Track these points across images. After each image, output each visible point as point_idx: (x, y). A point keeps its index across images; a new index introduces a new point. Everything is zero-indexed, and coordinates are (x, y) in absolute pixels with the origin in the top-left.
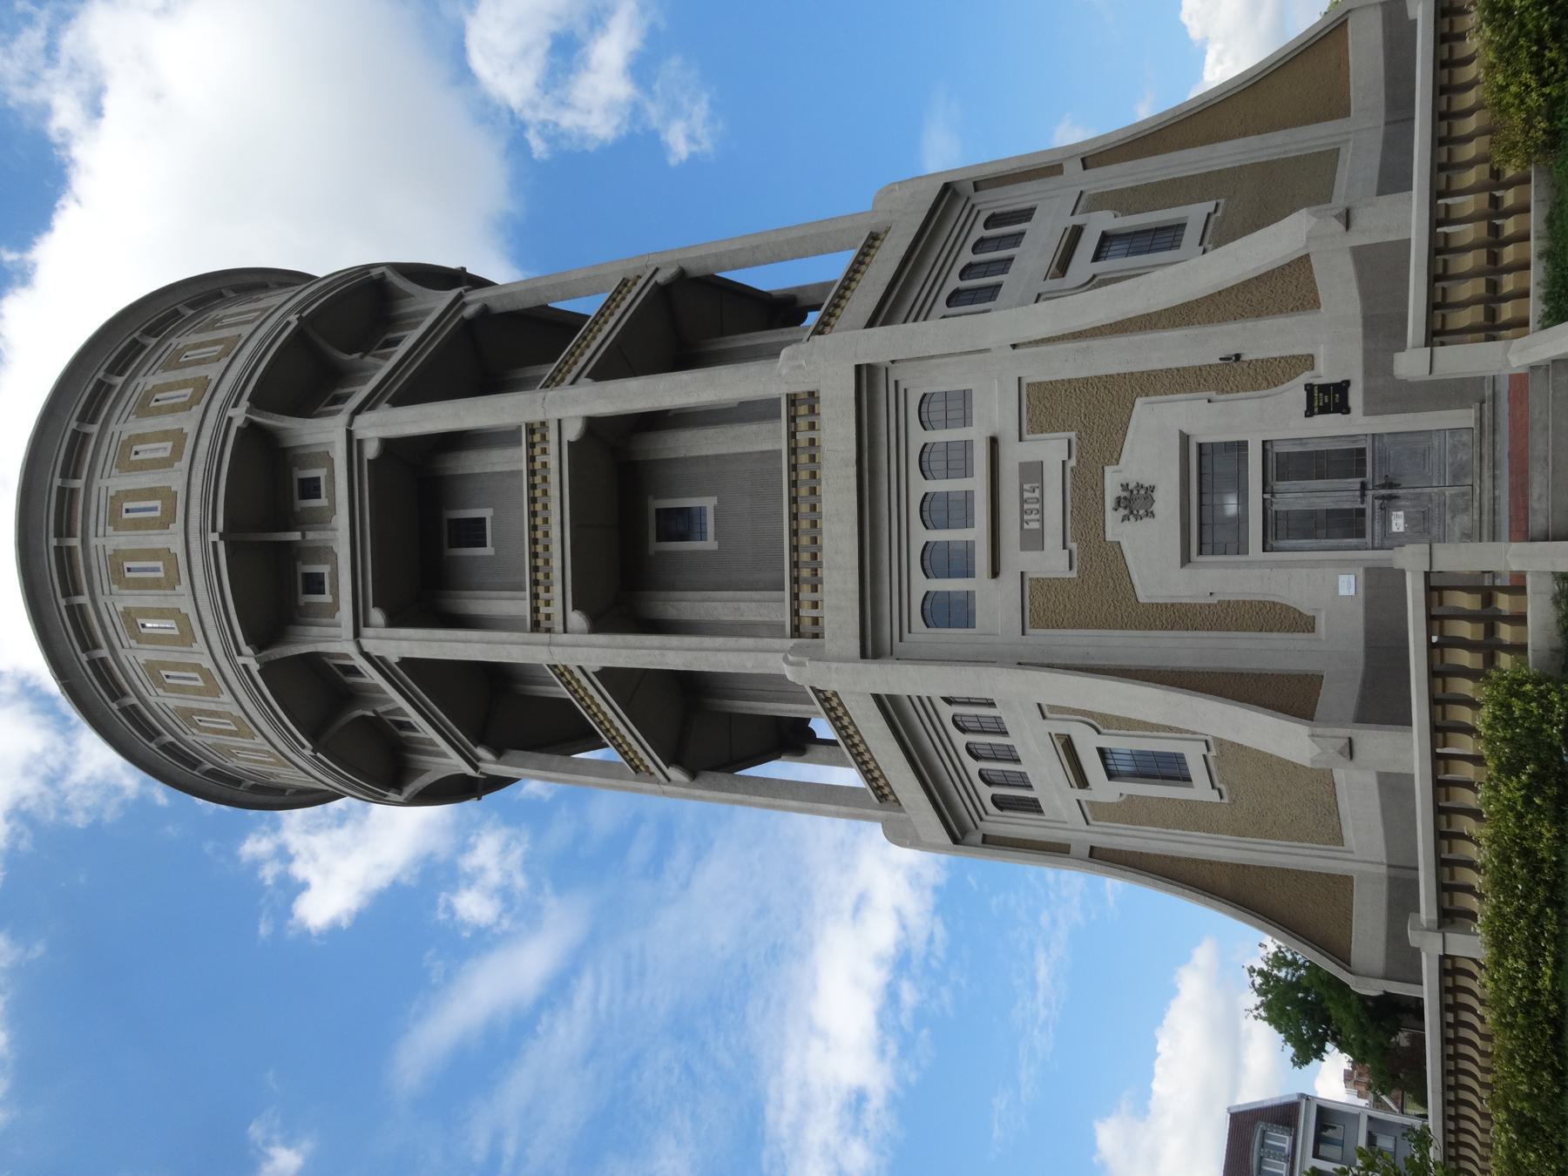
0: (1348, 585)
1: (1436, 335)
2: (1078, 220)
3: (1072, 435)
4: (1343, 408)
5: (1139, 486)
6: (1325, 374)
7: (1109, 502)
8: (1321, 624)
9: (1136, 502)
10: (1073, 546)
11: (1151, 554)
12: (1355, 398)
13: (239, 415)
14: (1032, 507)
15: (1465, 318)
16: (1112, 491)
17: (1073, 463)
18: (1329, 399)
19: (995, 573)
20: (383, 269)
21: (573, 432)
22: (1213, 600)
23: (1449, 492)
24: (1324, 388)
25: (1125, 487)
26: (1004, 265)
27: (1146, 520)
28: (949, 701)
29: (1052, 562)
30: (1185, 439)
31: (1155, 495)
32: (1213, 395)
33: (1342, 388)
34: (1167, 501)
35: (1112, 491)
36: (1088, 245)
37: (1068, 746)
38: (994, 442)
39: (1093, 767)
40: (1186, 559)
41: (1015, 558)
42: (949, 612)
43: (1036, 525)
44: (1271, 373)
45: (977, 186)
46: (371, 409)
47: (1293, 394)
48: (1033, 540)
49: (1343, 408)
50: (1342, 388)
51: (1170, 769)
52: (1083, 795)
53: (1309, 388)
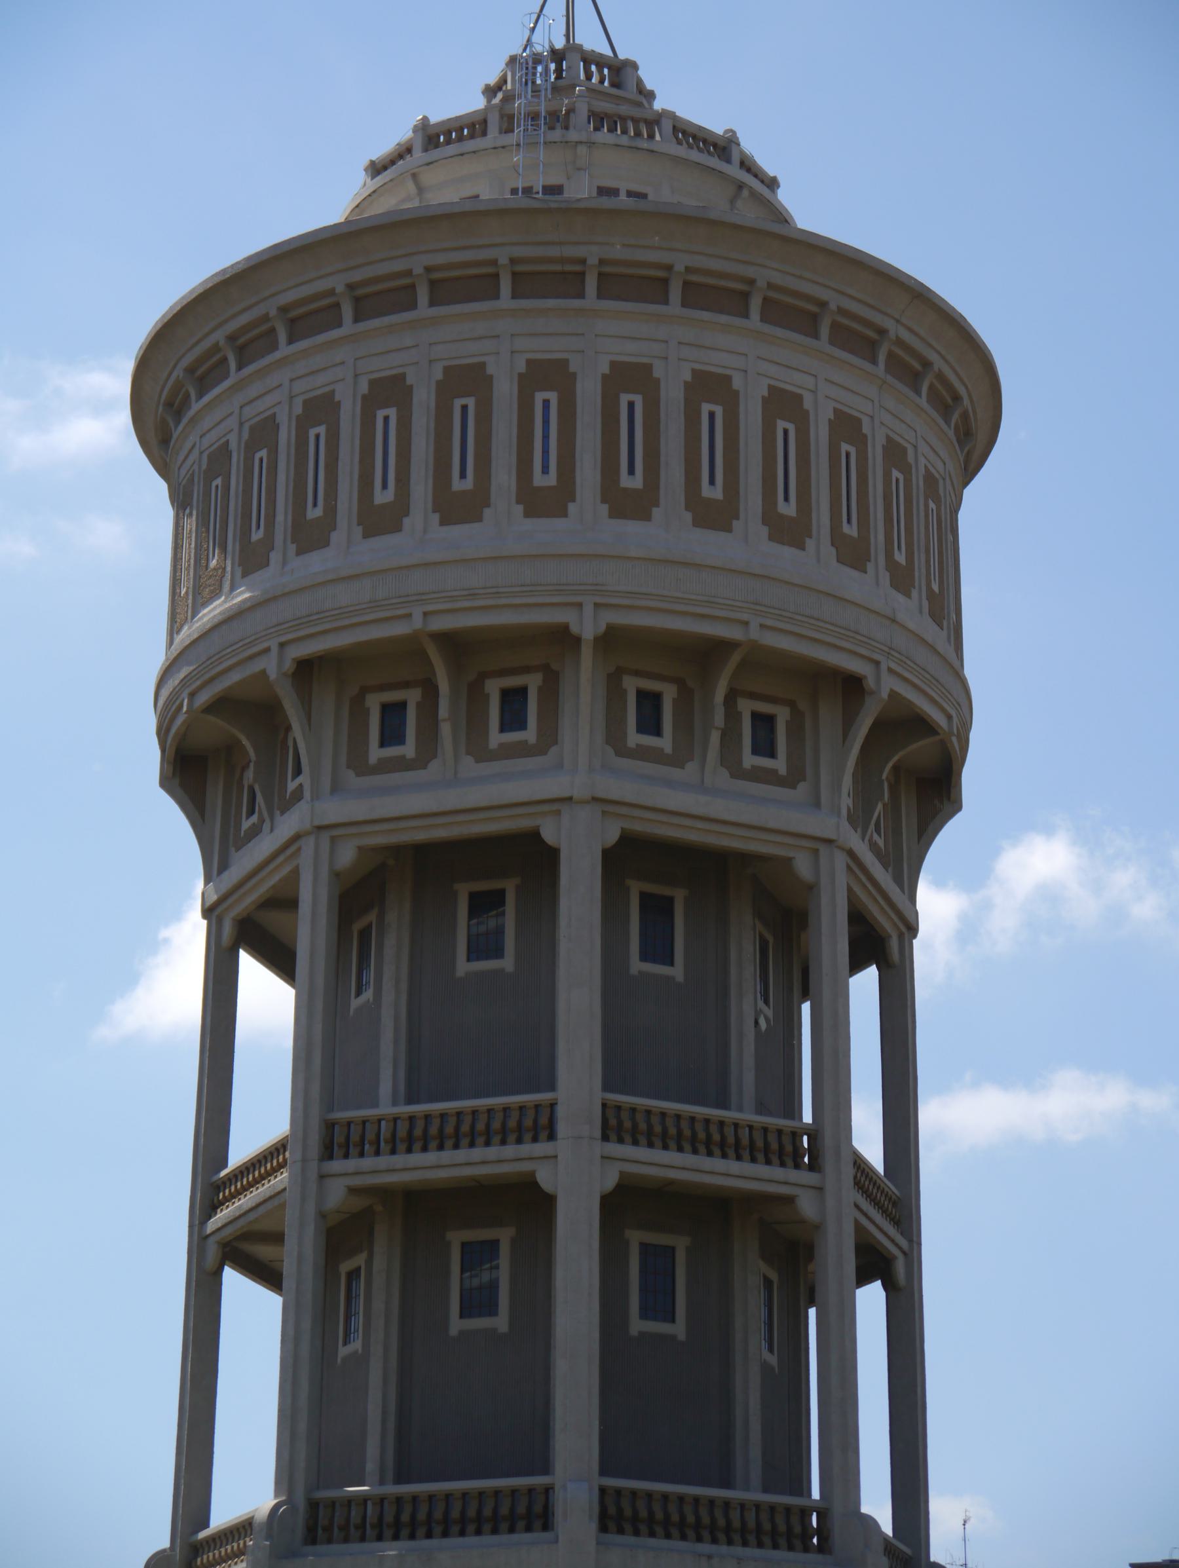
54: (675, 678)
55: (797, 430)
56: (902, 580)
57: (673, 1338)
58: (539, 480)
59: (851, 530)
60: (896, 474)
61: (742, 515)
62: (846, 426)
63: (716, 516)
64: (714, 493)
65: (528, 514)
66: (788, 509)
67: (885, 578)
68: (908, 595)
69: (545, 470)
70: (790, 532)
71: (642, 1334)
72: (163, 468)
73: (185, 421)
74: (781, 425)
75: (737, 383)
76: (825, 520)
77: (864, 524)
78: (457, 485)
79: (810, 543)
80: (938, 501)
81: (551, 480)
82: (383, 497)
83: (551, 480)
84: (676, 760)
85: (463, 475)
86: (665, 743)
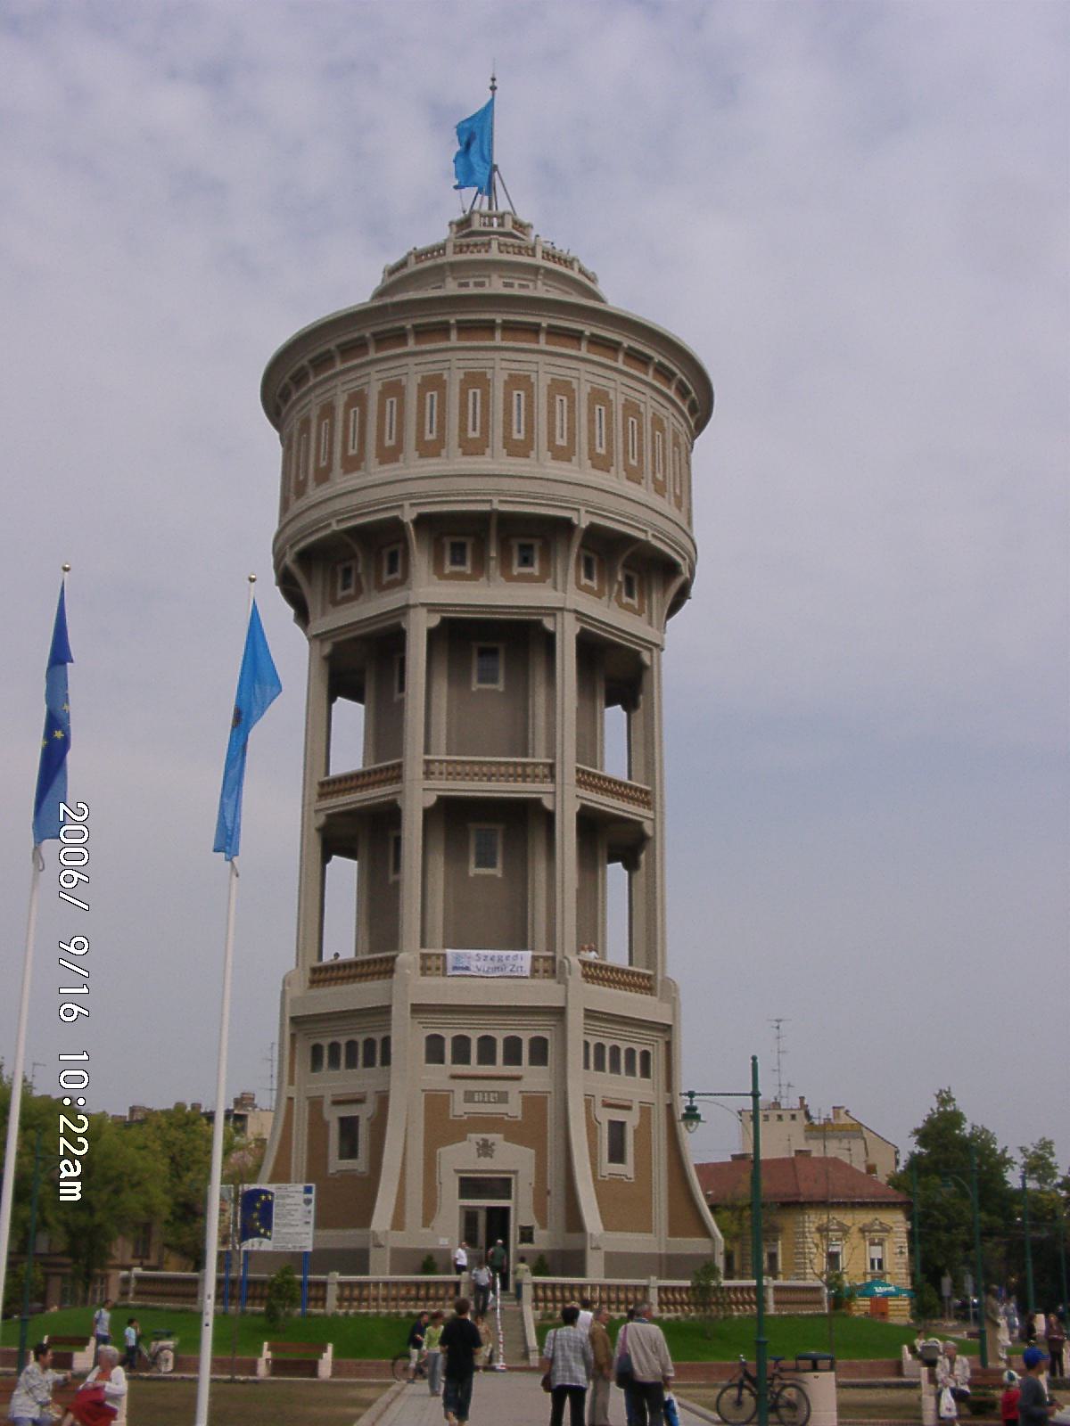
1: (536, 1286)
2: (636, 1107)
3: (520, 1119)
5: (493, 1151)
6: (538, 1233)
9: (485, 1149)
10: (465, 1117)
11: (460, 1157)
12: (525, 1246)
13: (583, 521)
14: (486, 1097)
15: (540, 1293)
17: (506, 1118)
18: (527, 1235)
19: (454, 1077)
20: (685, 569)
22: (438, 1184)
24: (531, 1234)
25: (493, 1144)
26: (615, 1068)
27: (476, 1155)
28: (386, 1042)
29: (459, 1108)
30: (515, 1172)
31: (488, 1158)
35: (491, 1137)
36: (618, 1116)
37: (359, 1101)
38: (518, 1078)
41: (460, 1088)
42: (434, 1050)
44: (540, 1210)
45: (668, 1044)
48: (469, 1097)
51: (349, 1151)
52: (327, 1101)
54: (528, 536)
55: (606, 410)
56: (660, 489)
57: (494, 877)
58: (471, 434)
59: (634, 462)
60: (657, 433)
61: (577, 453)
62: (631, 409)
65: (465, 454)
66: (601, 451)
67: (651, 486)
68: (664, 496)
71: (477, 876)
72: (278, 426)
73: (289, 403)
74: (598, 407)
75: (575, 386)
77: (640, 461)
78: (429, 437)
79: (613, 469)
80: (679, 448)
81: (477, 435)
82: (389, 443)
84: (541, 579)
86: (467, 569)
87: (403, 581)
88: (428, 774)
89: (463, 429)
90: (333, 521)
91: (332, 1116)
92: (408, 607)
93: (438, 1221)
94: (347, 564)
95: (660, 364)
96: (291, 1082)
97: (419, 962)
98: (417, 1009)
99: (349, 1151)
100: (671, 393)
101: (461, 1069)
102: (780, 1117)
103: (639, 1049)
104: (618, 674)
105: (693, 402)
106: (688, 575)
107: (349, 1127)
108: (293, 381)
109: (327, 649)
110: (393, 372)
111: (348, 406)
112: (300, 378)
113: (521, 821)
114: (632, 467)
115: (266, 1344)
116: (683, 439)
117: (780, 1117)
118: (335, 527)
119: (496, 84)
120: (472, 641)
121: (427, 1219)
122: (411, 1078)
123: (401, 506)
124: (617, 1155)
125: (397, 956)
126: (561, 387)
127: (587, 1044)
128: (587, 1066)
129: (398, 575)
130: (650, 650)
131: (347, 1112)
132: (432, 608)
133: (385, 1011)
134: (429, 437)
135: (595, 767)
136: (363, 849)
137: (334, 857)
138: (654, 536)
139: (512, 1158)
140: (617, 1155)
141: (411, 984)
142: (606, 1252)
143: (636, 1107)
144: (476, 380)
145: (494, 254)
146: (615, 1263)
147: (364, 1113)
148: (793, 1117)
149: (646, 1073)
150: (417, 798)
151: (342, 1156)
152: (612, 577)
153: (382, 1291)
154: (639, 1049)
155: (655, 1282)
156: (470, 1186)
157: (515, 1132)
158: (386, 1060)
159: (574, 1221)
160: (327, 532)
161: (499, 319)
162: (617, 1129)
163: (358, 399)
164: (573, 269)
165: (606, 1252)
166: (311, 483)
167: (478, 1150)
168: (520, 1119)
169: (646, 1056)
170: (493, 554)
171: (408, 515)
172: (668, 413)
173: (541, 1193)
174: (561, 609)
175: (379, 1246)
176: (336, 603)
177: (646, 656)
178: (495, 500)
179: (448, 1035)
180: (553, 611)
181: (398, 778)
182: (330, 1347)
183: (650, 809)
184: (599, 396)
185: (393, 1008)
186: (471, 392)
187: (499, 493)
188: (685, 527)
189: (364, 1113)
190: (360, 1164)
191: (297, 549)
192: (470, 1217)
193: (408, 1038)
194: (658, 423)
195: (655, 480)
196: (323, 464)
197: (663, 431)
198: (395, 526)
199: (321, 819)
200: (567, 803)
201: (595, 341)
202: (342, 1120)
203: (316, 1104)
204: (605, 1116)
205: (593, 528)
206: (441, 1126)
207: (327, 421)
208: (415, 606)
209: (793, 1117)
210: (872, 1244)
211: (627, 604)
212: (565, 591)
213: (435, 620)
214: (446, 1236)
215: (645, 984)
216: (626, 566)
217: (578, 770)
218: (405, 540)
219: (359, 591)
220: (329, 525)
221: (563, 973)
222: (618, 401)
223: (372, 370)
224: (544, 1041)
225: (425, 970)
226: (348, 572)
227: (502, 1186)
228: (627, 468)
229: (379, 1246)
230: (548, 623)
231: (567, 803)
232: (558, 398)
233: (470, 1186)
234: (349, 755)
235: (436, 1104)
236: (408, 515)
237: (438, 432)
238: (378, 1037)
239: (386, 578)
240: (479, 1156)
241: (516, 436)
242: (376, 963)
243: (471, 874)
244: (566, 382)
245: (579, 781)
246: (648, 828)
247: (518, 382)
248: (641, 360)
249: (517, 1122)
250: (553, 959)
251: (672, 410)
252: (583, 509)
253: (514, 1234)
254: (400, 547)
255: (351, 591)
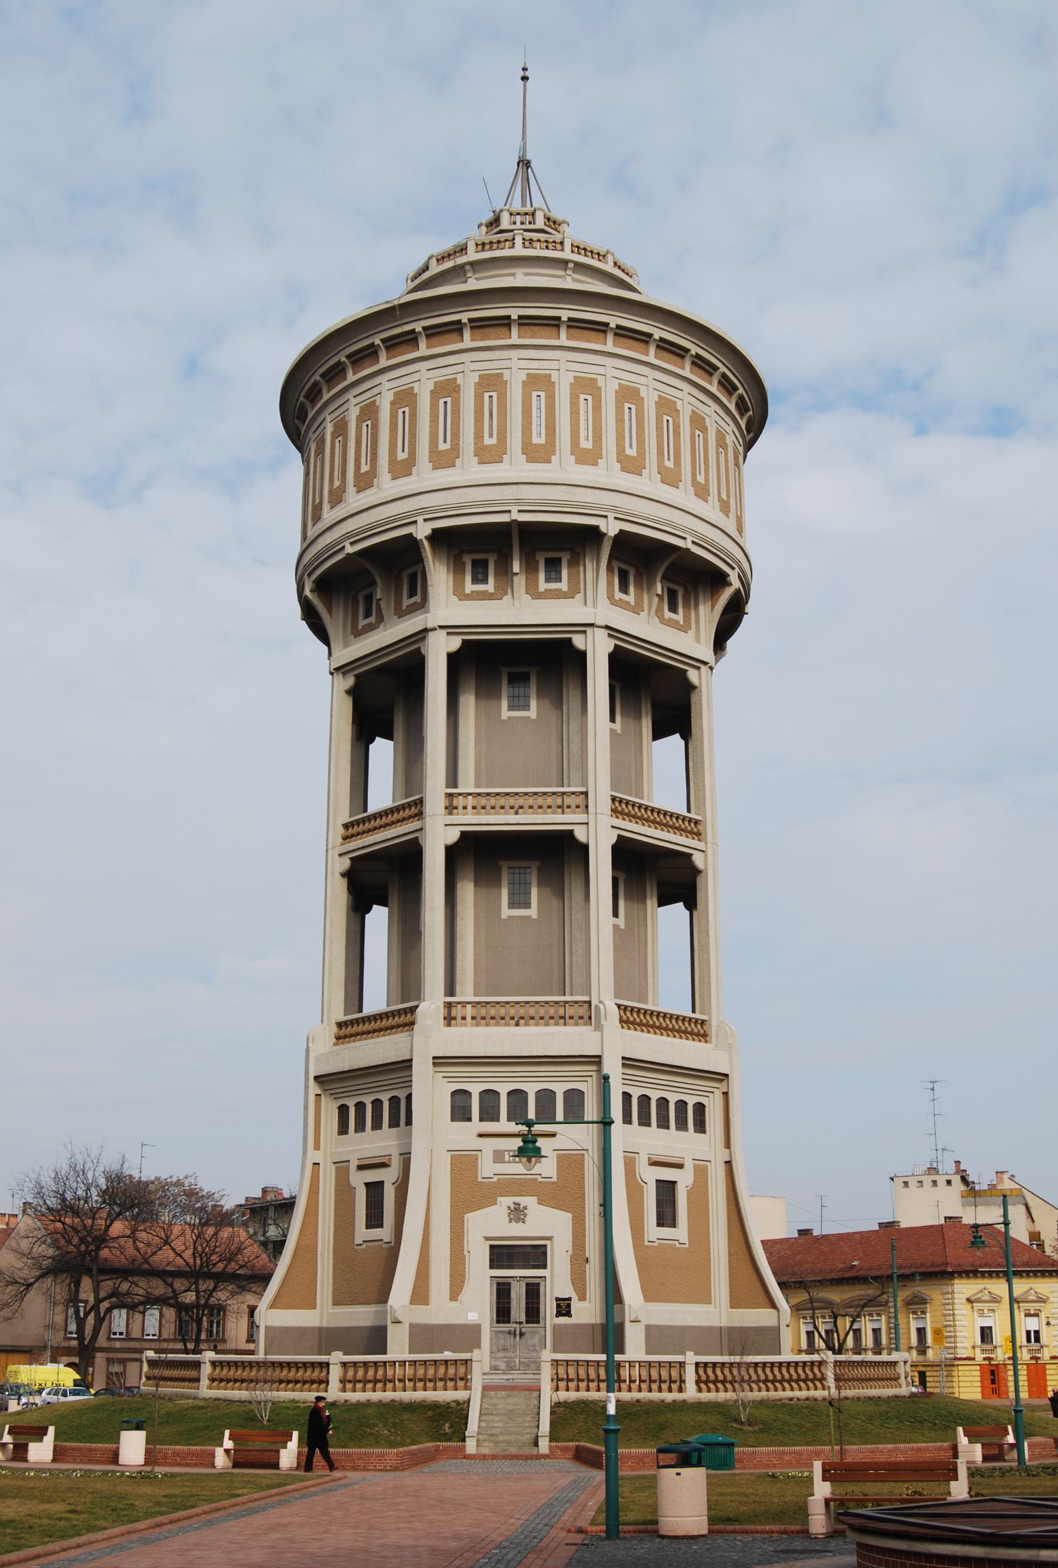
0: (472, 1317)
1: (556, 1363)
2: (689, 1165)
3: (555, 1179)
4: (559, 1314)
5: (525, 1215)
6: (575, 1305)
7: (517, 1199)
8: (454, 1304)
9: (517, 1214)
10: (495, 1179)
11: (490, 1223)
12: (563, 1320)
13: (611, 528)
16: (523, 1201)
17: (540, 1179)
18: (564, 1308)
21: (580, 834)
22: (466, 1253)
23: (517, 1363)
24: (569, 1306)
25: (525, 1208)
28: (409, 1097)
29: (488, 1169)
30: (550, 1238)
31: (521, 1223)
32: (570, 1252)
33: (568, 1314)
34: (517, 1230)
35: (523, 1201)
36: (667, 1174)
39: (372, 1176)
40: (487, 1239)
41: (490, 1145)
42: (460, 1111)
43: (507, 1158)
46: (609, 635)
47: (566, 1290)
49: (559, 1314)
50: (568, 1314)
53: (569, 1299)
59: (670, 464)
61: (604, 456)
63: (588, 458)
64: (586, 444)
65: (481, 462)
66: (632, 452)
69: (491, 435)
70: (632, 466)
74: (627, 405)
76: (654, 458)
78: (442, 446)
81: (494, 441)
82: (401, 456)
83: (494, 441)
84: (569, 595)
85: (445, 441)
87: (422, 605)
88: (450, 809)
89: (479, 436)
90: (347, 544)
91: (359, 1180)
92: (426, 630)
93: (465, 1295)
94: (367, 592)
95: (698, 356)
96: (317, 1147)
97: (442, 1012)
98: (439, 1061)
99: (374, 1219)
100: (714, 388)
101: (490, 1127)
102: (935, 1183)
103: (691, 1101)
104: (658, 694)
105: (741, 398)
106: (736, 584)
107: (375, 1189)
108: (308, 395)
109: (350, 681)
110: (405, 380)
111: (360, 419)
112: (314, 394)
113: (554, 855)
114: (666, 468)
115: (227, 1432)
116: (730, 439)
117: (935, 1183)
118: (350, 549)
119: (528, 74)
120: (486, 662)
121: (454, 1295)
122: (436, 1136)
123: (416, 522)
124: (666, 1216)
125: (417, 1007)
126: (585, 386)
127: (627, 1096)
128: (627, 1119)
129: (417, 599)
130: (698, 668)
131: (372, 1176)
132: (451, 629)
133: (405, 1065)
134: (442, 446)
135: (642, 798)
136: (394, 897)
137: (375, 907)
138: (693, 542)
139: (547, 1223)
140: (666, 1216)
141: (432, 1036)
142: (648, 1328)
143: (689, 1165)
144: (492, 382)
145: (519, 250)
146: (656, 1337)
147: (388, 1177)
148: (949, 1182)
149: (700, 1126)
150: (438, 835)
151: (369, 1226)
152: (651, 585)
153: (409, 1371)
154: (691, 1101)
155: (691, 1358)
156: (502, 1255)
157: (554, 1195)
158: (409, 1122)
159: (613, 1294)
160: (340, 556)
161: (514, 314)
162: (666, 1190)
163: (369, 412)
164: (606, 263)
165: (648, 1328)
166: (326, 506)
167: (509, 1214)
168: (555, 1179)
169: (700, 1108)
170: (516, 567)
171: (422, 531)
172: (711, 413)
173: (579, 1260)
174: (592, 625)
175: (397, 1322)
176: (358, 633)
177: (693, 675)
178: (514, 509)
179: (475, 1089)
180: (583, 628)
181: (420, 815)
182: (295, 1434)
183: (699, 840)
184: (628, 394)
185: (414, 1063)
186: (487, 395)
187: (518, 501)
188: (733, 531)
189: (388, 1177)
190: (385, 1233)
191: (314, 577)
192: (503, 1291)
193: (431, 1094)
194: (698, 422)
195: (695, 483)
196: (337, 483)
197: (704, 429)
198: (410, 544)
199: (346, 863)
200: (600, 838)
201: (622, 333)
202: (368, 1185)
203: (342, 1168)
204: (651, 1176)
205: (623, 537)
206: (469, 1191)
207: (340, 438)
208: (435, 629)
209: (949, 1182)
210: (1027, 1315)
211: (670, 619)
212: (595, 606)
213: (455, 644)
214: (476, 1307)
215: (694, 1029)
216: (664, 578)
217: (614, 799)
218: (420, 560)
219: (380, 618)
220: (343, 548)
221: (598, 1020)
222: (650, 398)
223: (383, 378)
224: (581, 1094)
225: (449, 1020)
226: (369, 599)
227: (535, 1255)
228: (661, 470)
229: (397, 1322)
230: (578, 641)
231: (600, 838)
232: (582, 397)
233: (502, 1255)
234: (382, 794)
235: (463, 1164)
236: (422, 531)
237: (452, 441)
238: (402, 1094)
239: (406, 602)
240: (510, 1221)
241: (536, 440)
242: (400, 1019)
243: (504, 916)
244: (591, 379)
245: (614, 810)
246: (698, 860)
247: (538, 382)
248: (708, 369)
249: (553, 1183)
250: (589, 1003)
251: (715, 407)
252: (611, 516)
253: (548, 1307)
254: (418, 568)
255: (372, 619)
